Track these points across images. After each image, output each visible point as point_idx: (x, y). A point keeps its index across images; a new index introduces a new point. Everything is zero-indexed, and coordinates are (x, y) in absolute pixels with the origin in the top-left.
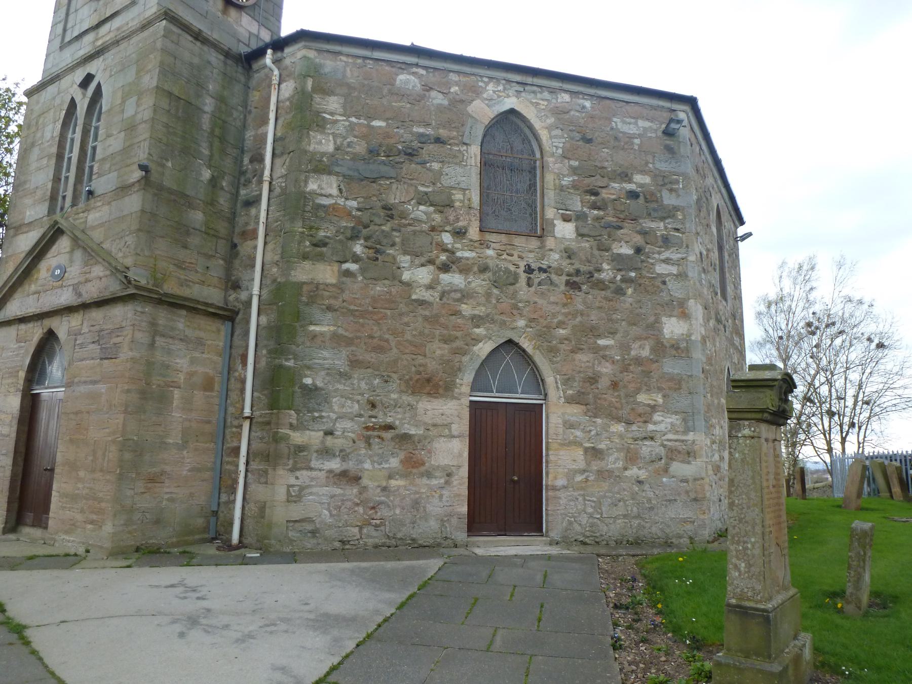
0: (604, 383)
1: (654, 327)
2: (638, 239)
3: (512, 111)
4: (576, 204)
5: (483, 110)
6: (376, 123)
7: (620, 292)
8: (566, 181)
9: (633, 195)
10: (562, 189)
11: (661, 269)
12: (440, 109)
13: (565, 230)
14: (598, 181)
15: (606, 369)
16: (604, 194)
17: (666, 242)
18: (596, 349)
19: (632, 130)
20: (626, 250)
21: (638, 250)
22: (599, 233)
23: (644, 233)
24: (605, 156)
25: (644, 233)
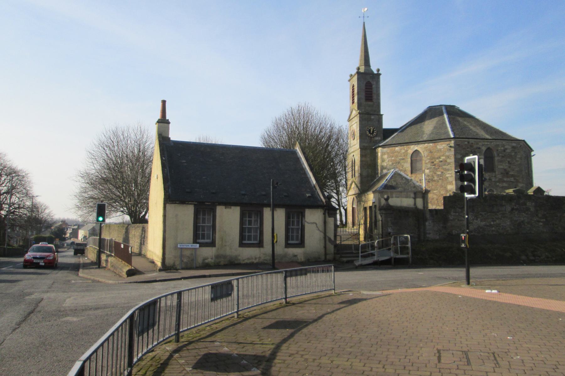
0: (435, 199)
1: (446, 188)
2: (442, 170)
3: (416, 150)
4: (429, 166)
5: (410, 151)
6: (393, 158)
7: (438, 181)
8: (427, 161)
9: (441, 161)
10: (426, 163)
11: (447, 175)
12: (404, 153)
13: (427, 171)
14: (433, 160)
15: (435, 196)
16: (435, 162)
17: (448, 170)
18: (434, 193)
19: (442, 147)
20: (439, 173)
21: (442, 173)
22: (434, 171)
23: (443, 169)
24: (436, 155)
25: (443, 169)
